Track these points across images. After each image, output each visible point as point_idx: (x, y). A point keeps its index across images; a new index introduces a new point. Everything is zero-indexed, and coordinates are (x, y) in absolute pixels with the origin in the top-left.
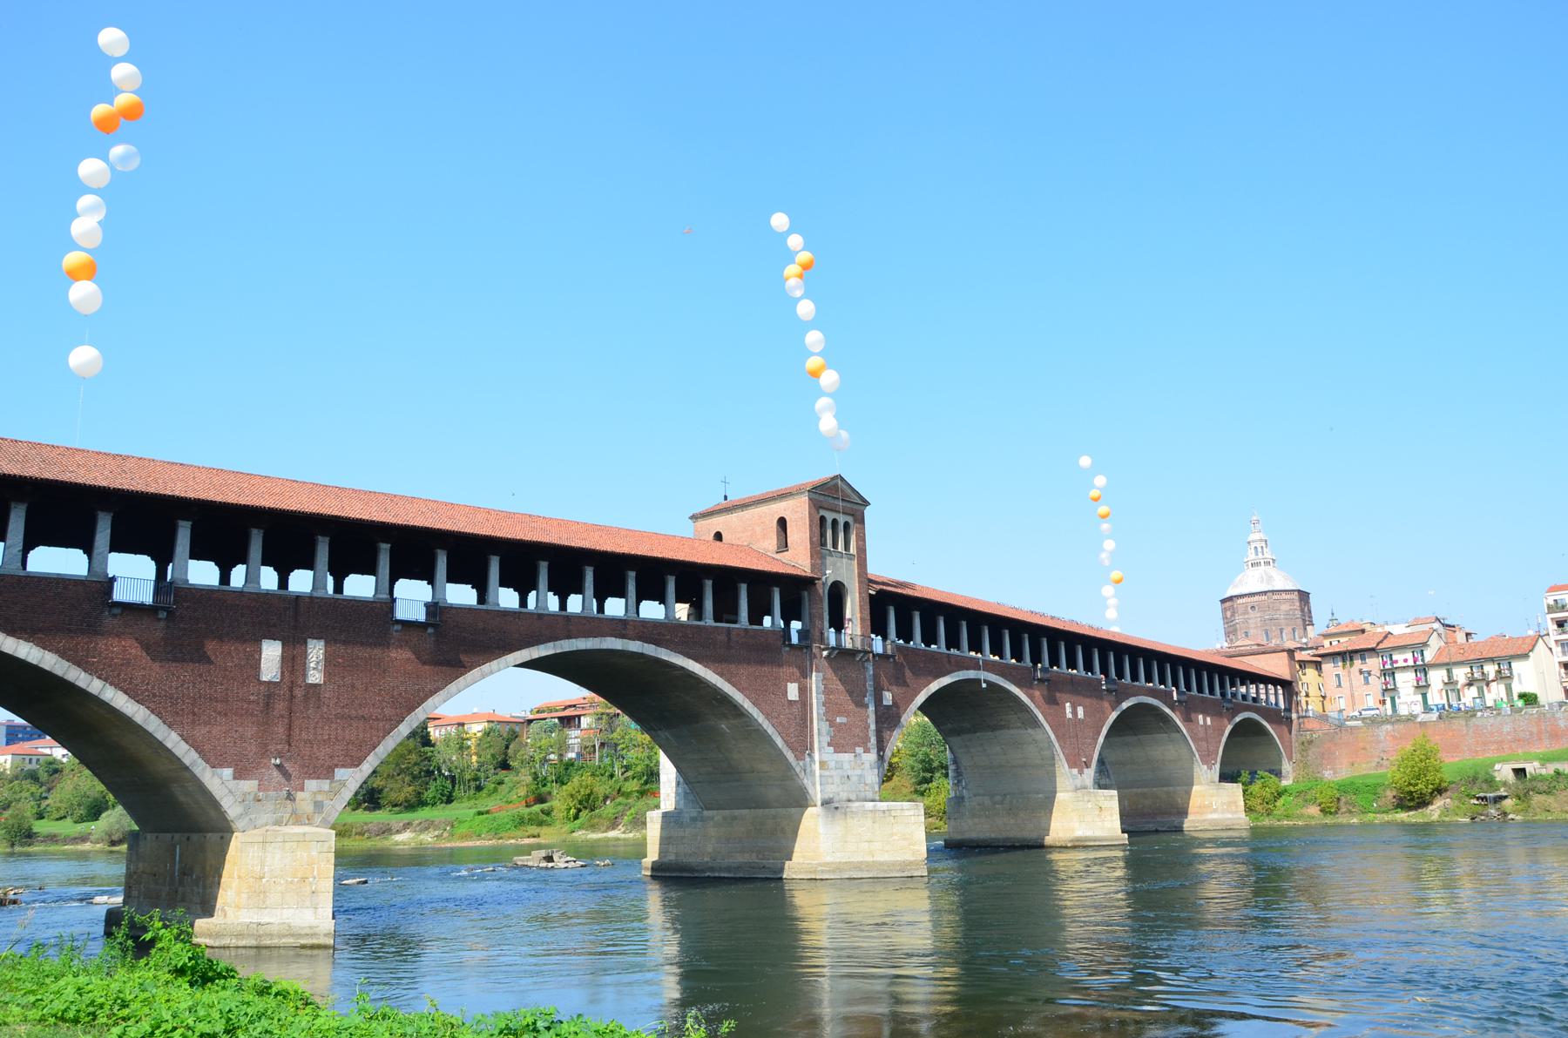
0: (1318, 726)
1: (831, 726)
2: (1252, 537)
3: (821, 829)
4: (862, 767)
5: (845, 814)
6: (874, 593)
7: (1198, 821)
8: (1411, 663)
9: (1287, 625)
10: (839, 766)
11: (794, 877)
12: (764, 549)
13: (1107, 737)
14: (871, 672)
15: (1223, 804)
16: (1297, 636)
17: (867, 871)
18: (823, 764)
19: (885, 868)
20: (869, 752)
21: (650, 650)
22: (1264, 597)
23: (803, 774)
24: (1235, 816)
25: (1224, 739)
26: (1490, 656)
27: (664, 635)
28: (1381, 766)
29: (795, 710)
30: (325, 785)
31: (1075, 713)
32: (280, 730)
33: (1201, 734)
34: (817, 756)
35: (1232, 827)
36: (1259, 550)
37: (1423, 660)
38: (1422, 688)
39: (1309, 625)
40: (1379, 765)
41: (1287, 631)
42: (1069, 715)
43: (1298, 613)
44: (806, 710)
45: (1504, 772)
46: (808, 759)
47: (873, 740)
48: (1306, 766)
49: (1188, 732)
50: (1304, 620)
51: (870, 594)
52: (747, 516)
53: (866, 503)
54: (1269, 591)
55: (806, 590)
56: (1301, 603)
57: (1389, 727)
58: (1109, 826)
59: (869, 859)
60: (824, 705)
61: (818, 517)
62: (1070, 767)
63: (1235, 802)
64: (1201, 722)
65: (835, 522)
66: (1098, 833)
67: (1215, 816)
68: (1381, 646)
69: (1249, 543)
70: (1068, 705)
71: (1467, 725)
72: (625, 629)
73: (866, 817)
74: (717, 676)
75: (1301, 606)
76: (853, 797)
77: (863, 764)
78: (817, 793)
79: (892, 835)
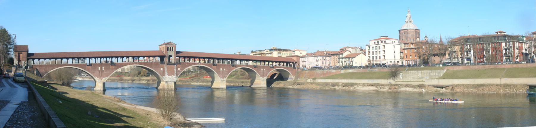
18: (166, 77)
31: (223, 69)
32: (100, 74)
36: (409, 18)
39: (418, 37)
43: (415, 35)
47: (175, 74)
53: (176, 45)
65: (170, 48)
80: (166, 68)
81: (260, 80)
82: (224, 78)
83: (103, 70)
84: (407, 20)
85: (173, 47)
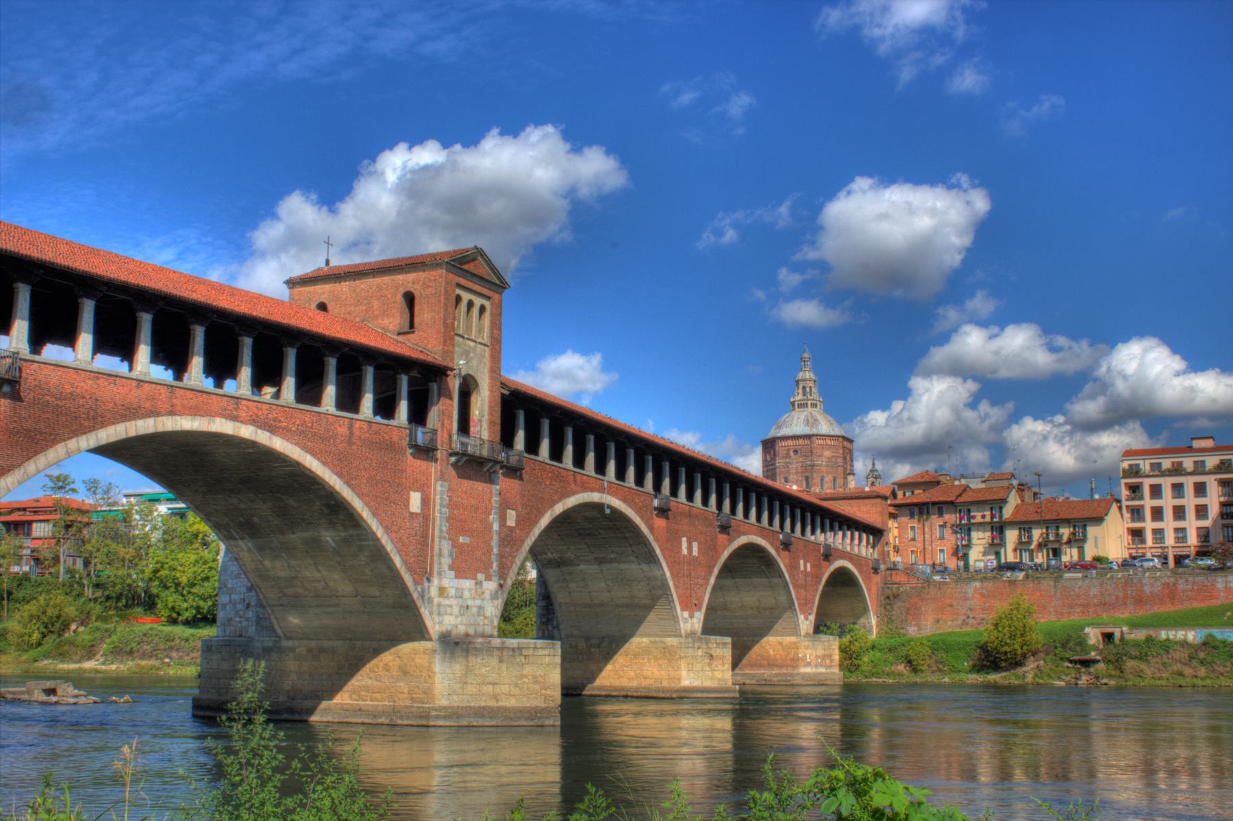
0: (906, 580)
1: (453, 546)
2: (801, 375)
3: (438, 667)
4: (483, 597)
5: (467, 651)
6: (507, 393)
7: (792, 675)
8: (988, 519)
9: (828, 473)
10: (460, 596)
11: (399, 722)
12: (383, 328)
13: (719, 577)
15: (817, 657)
16: (837, 485)
17: (491, 718)
18: (442, 591)
19: (512, 715)
20: (490, 580)
21: (263, 438)
22: (807, 442)
23: (421, 601)
24: (829, 671)
25: (821, 588)
26: (1068, 517)
27: (280, 422)
28: (967, 624)
29: (416, 524)
31: (690, 549)
33: (801, 582)
34: (435, 581)
35: (825, 682)
36: (808, 390)
37: (1001, 517)
38: (995, 546)
39: (849, 474)
40: (964, 623)
41: (829, 478)
42: (685, 551)
43: (840, 461)
44: (427, 525)
45: (1093, 636)
46: (426, 584)
48: (890, 620)
49: (790, 577)
50: (845, 469)
51: (502, 394)
52: (362, 286)
54: (813, 435)
55: (436, 381)
56: (844, 451)
57: (978, 584)
58: (719, 676)
59: (493, 704)
60: (448, 520)
61: (454, 296)
62: (682, 610)
63: (830, 656)
64: (802, 568)
65: (470, 304)
66: (708, 684)
67: (808, 670)
68: (961, 500)
69: (797, 382)
70: (684, 539)
71: (1055, 586)
72: (237, 409)
73: (492, 656)
74: (335, 477)
75: (843, 454)
76: (471, 631)
77: (483, 593)
78: (436, 624)
79: (522, 676)
80: (439, 490)
81: (796, 632)
84: (800, 397)
85: (487, 304)
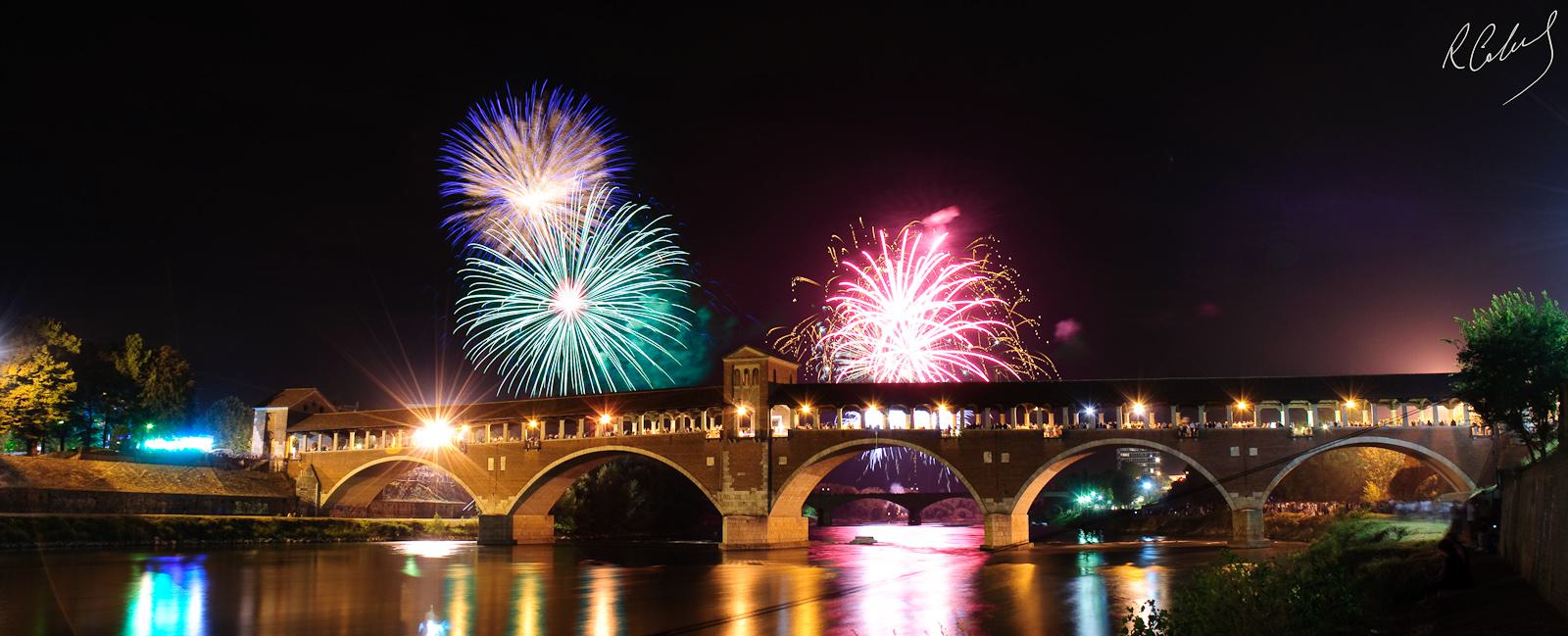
10: (739, 497)
14: (767, 448)
21: (627, 449)
30: (506, 501)
31: (996, 457)
47: (765, 484)
65: (746, 371)
82: (1005, 500)
83: (503, 468)
